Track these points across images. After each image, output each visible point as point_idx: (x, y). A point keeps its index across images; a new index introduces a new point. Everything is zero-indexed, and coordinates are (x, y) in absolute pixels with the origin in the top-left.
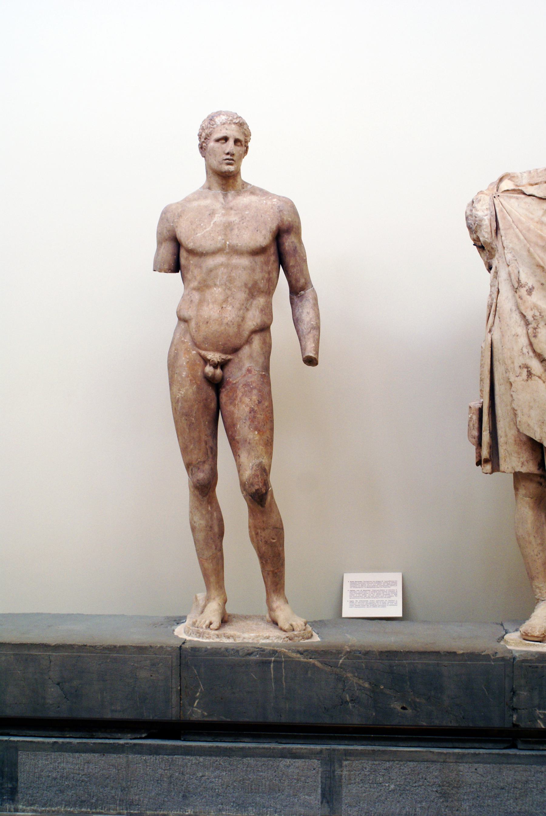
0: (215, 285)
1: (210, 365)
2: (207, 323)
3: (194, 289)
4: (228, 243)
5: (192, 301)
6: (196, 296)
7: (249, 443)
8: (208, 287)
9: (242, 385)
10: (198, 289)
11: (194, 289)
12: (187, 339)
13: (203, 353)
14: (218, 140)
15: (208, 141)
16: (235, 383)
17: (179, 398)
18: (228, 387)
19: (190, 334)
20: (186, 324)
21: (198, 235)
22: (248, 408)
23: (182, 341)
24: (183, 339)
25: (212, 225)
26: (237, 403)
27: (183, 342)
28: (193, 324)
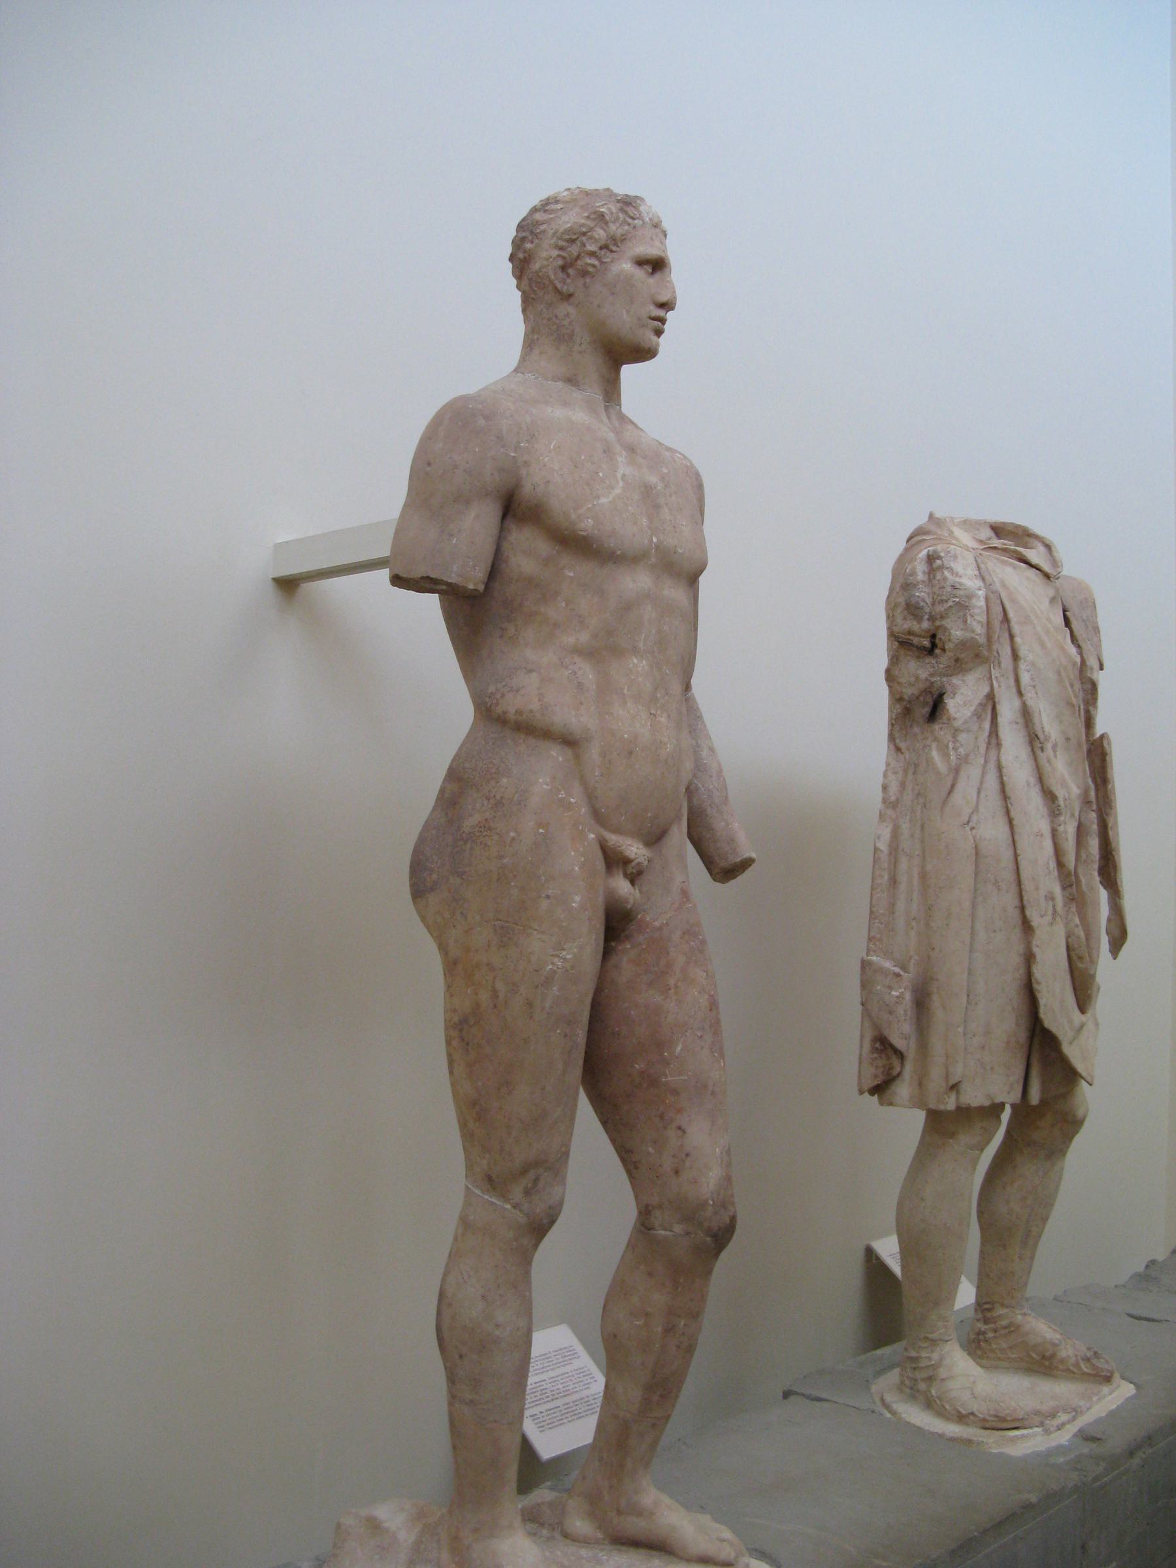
0: (635, 651)
1: (626, 875)
2: (630, 753)
3: (578, 651)
4: (655, 540)
5: (580, 685)
6: (587, 672)
7: (713, 1093)
8: (617, 651)
9: (679, 933)
10: (591, 654)
11: (578, 651)
12: (576, 797)
13: (613, 839)
14: (641, 262)
15: (608, 253)
16: (660, 928)
17: (553, 972)
18: (641, 938)
19: (584, 782)
20: (569, 752)
21: (603, 500)
22: (706, 997)
23: (561, 800)
24: (562, 795)
25: (621, 484)
26: (672, 982)
27: (568, 806)
28: (593, 753)
